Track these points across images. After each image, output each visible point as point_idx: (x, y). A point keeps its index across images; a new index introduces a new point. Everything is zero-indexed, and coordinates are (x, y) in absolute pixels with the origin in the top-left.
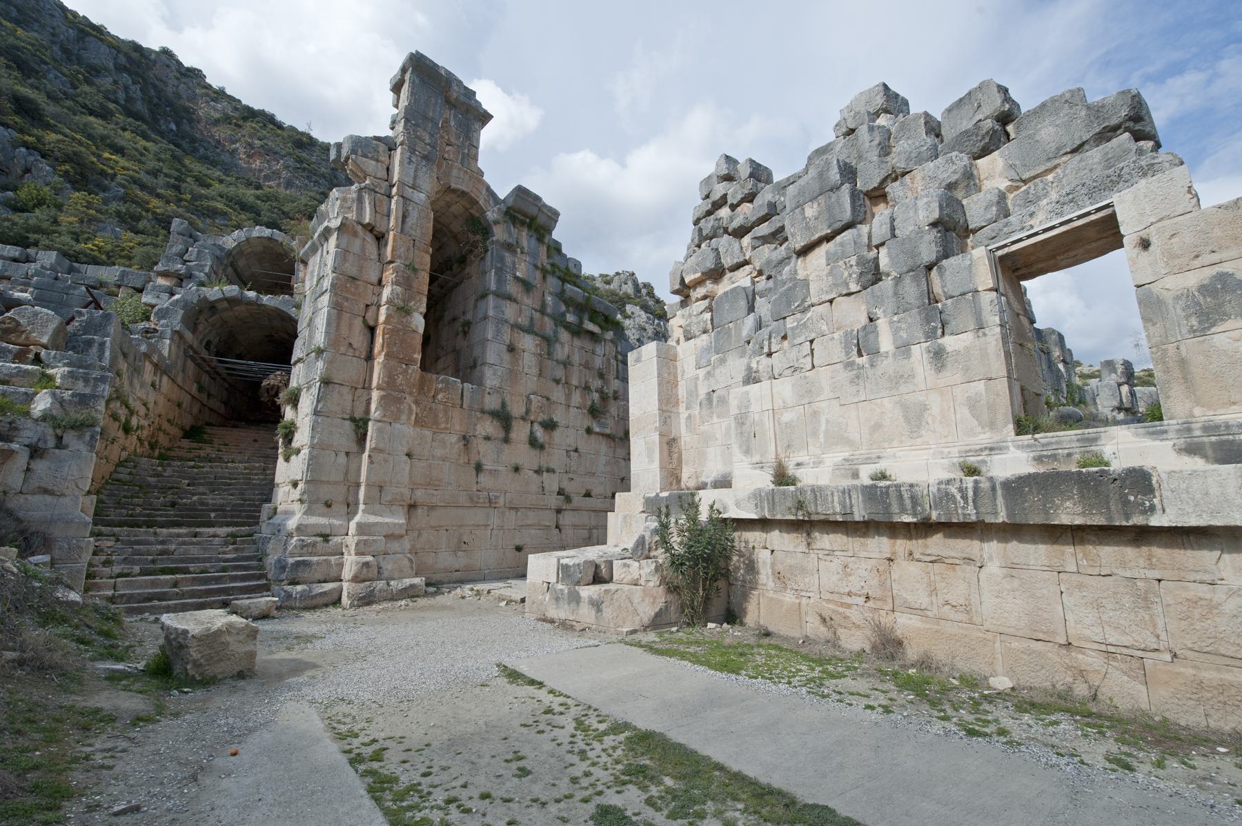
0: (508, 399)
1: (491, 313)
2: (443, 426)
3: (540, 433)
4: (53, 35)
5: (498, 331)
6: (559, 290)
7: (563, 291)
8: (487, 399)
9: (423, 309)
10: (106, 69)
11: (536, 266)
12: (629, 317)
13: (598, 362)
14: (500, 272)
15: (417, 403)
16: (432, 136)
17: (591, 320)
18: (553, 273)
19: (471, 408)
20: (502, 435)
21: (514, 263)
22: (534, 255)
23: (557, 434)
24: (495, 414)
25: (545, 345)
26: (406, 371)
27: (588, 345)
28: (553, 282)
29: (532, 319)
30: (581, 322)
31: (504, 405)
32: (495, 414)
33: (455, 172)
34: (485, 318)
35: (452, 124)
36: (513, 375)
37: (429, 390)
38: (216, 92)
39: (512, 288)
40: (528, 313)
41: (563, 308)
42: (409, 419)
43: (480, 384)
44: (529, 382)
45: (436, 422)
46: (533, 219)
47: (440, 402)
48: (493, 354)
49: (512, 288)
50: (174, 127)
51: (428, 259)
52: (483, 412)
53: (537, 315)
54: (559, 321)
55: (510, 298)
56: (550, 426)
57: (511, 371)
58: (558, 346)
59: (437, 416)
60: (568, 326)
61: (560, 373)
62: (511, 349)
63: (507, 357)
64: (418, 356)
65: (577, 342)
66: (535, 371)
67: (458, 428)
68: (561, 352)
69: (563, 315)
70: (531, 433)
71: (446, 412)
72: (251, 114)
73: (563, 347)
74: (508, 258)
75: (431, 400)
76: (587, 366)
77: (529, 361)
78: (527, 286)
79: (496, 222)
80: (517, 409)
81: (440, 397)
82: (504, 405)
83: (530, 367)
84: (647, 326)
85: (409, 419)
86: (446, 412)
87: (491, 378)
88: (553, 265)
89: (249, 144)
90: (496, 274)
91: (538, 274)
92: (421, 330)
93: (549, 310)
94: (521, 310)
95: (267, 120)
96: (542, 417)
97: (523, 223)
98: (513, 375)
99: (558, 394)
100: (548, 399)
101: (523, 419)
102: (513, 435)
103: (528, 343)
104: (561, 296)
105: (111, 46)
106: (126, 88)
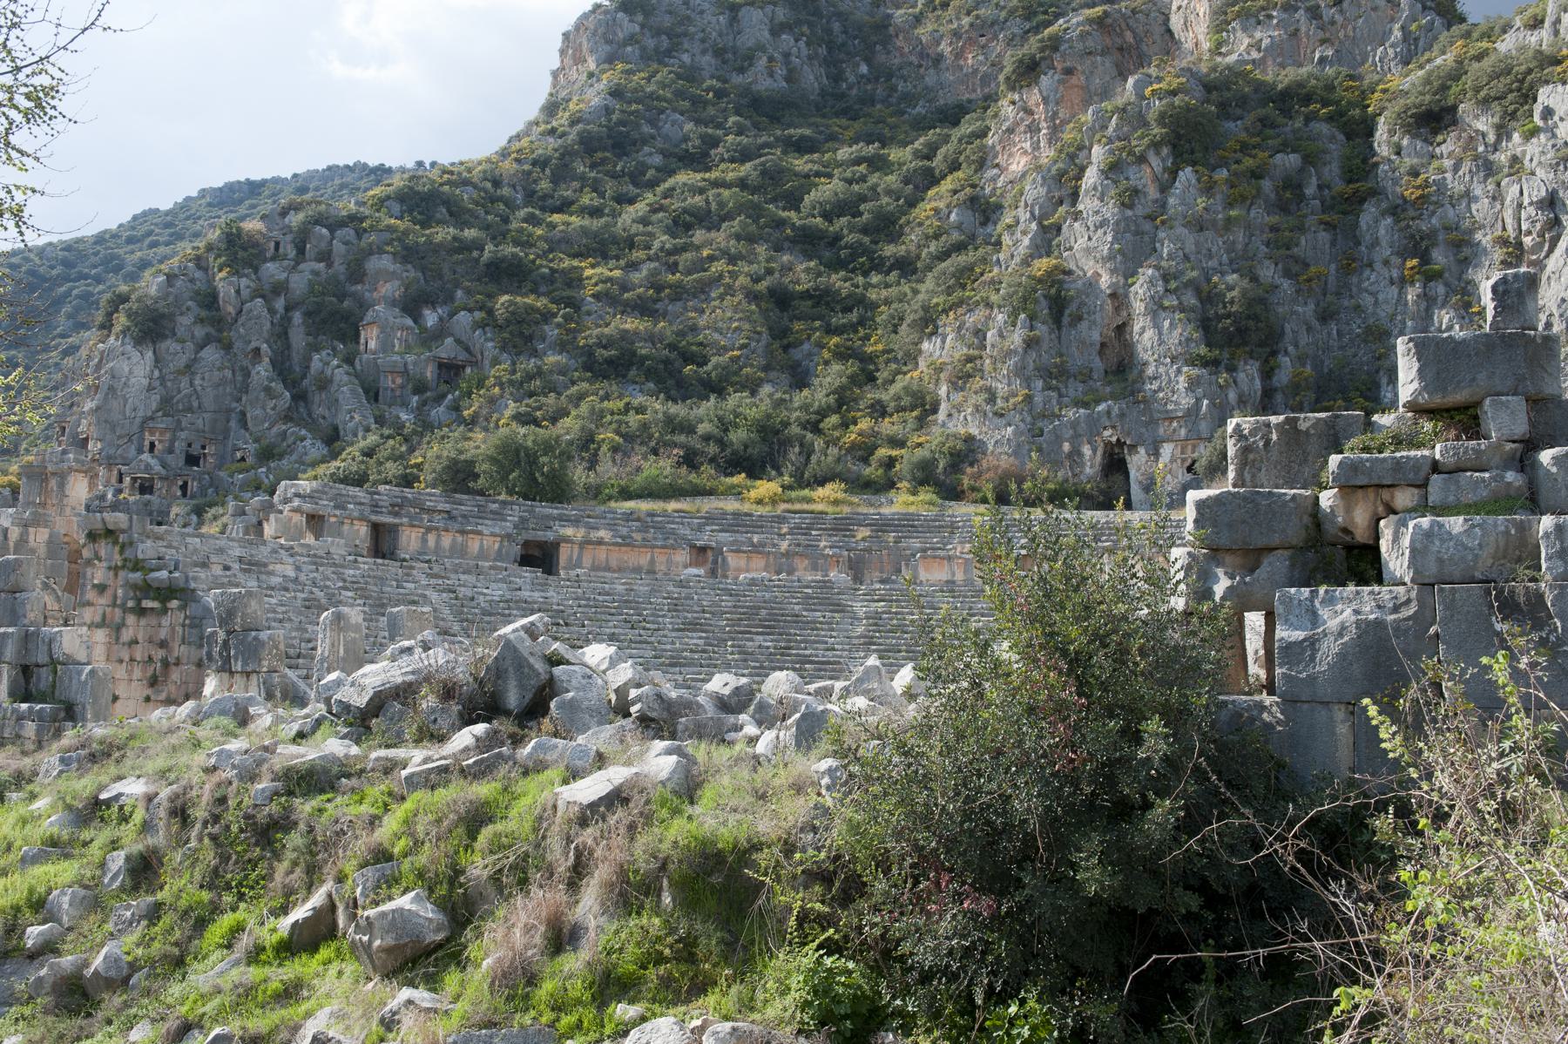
4: (703, 41)
10: (761, 48)
11: (110, 568)
12: (1534, 132)
13: (163, 634)
18: (123, 567)
29: (104, 615)
40: (100, 612)
49: (90, 595)
50: (864, 69)
53: (108, 610)
55: (89, 604)
58: (124, 630)
60: (132, 610)
65: (143, 622)
66: (103, 658)
68: (126, 635)
78: (101, 589)
89: (956, 34)
103: (101, 635)
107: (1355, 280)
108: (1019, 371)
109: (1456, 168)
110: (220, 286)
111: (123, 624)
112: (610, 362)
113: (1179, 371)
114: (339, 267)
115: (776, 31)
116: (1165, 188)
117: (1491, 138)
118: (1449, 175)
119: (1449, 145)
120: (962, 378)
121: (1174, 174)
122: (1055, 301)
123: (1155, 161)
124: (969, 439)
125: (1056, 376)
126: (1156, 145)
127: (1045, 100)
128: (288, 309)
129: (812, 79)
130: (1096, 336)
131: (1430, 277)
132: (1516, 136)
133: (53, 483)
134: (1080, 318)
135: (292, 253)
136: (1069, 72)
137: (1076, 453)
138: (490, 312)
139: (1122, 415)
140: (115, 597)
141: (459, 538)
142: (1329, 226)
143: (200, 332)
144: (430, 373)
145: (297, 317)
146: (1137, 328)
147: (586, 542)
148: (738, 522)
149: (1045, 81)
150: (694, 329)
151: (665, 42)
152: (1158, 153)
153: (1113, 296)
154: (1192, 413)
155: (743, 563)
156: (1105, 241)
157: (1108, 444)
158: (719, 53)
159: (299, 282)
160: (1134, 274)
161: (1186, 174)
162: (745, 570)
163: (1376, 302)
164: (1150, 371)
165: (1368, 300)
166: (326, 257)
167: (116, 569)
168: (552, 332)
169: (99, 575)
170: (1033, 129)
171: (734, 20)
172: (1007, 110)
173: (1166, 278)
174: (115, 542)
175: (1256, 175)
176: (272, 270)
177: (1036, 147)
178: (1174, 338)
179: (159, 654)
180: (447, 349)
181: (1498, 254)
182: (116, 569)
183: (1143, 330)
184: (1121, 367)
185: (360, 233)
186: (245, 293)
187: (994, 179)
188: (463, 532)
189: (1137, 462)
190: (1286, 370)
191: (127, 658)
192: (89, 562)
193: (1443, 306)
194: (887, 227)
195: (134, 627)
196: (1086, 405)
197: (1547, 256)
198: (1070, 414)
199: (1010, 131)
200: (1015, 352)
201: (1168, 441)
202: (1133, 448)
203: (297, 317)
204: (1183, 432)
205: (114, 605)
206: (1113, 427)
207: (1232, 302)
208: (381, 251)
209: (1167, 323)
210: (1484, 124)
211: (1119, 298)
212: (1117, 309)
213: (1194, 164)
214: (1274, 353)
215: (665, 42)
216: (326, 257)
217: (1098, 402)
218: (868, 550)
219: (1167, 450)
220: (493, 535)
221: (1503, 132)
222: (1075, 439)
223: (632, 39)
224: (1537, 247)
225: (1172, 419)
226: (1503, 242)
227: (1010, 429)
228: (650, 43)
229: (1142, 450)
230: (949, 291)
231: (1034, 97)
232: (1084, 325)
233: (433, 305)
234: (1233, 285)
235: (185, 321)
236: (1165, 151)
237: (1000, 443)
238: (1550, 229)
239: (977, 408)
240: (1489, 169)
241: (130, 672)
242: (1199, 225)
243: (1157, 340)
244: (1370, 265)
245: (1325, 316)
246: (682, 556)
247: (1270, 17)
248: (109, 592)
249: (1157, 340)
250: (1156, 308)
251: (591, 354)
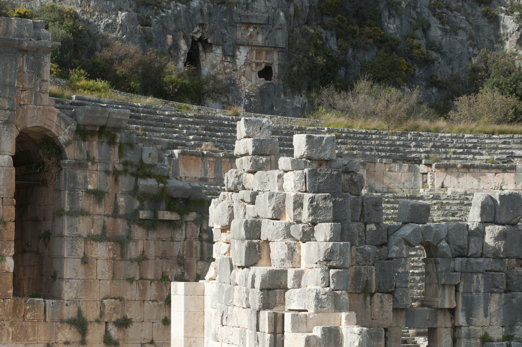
0: (83, 308)
1: (66, 233)
2: (31, 339)
3: (114, 332)
5: (73, 248)
6: (131, 188)
7: (136, 187)
8: (66, 310)
9: (12, 253)
11: (107, 172)
13: (178, 248)
14: (73, 191)
15: (12, 324)
16: (10, 99)
17: (169, 208)
18: (125, 172)
19: (52, 321)
20: (78, 338)
21: (85, 178)
22: (105, 161)
23: (131, 331)
24: (71, 322)
25: (118, 248)
26: (3, 304)
27: (165, 234)
28: (126, 182)
29: (104, 227)
30: (156, 215)
31: (80, 312)
32: (71, 322)
33: (30, 114)
34: (62, 236)
35: (25, 69)
36: (87, 284)
37: (20, 312)
39: (85, 203)
40: (99, 222)
41: (137, 204)
42: (8, 339)
43: (59, 298)
44: (104, 286)
45: (27, 337)
46: (102, 128)
47: (29, 320)
48: (70, 269)
49: (85, 203)
51: (13, 209)
52: (62, 321)
53: (109, 221)
54: (132, 218)
55: (83, 213)
56: (124, 323)
57: (85, 281)
58: (132, 246)
59: (27, 331)
60: (142, 223)
61: (134, 271)
62: (85, 261)
63: (81, 269)
64: (11, 291)
65: (153, 235)
66: (108, 275)
67: (43, 338)
68: (134, 250)
69: (136, 212)
70: (106, 331)
71: (33, 327)
73: (136, 242)
74: (80, 174)
75: (21, 320)
76: (164, 256)
77: (102, 268)
78: (98, 195)
79: (68, 143)
80: (91, 314)
81: (28, 316)
82: (80, 312)
83: (103, 273)
85: (8, 339)
86: (33, 327)
87: (68, 292)
88: (125, 164)
90: (69, 194)
91: (110, 179)
92: (12, 270)
93: (121, 212)
94: (93, 221)
96: (115, 317)
97: (92, 134)
98: (87, 284)
99: (132, 292)
100: (121, 299)
101: (98, 321)
102: (89, 337)
103: (101, 251)
104: (134, 192)
111: (129, 237)
140: (116, 207)
167: (116, 174)
174: (111, 142)
182: (116, 174)
189: (212, 62)
202: (208, 46)
204: (260, 38)
205: (115, 214)
219: (242, 55)
227: (122, 15)
241: (143, 292)
248: (108, 200)
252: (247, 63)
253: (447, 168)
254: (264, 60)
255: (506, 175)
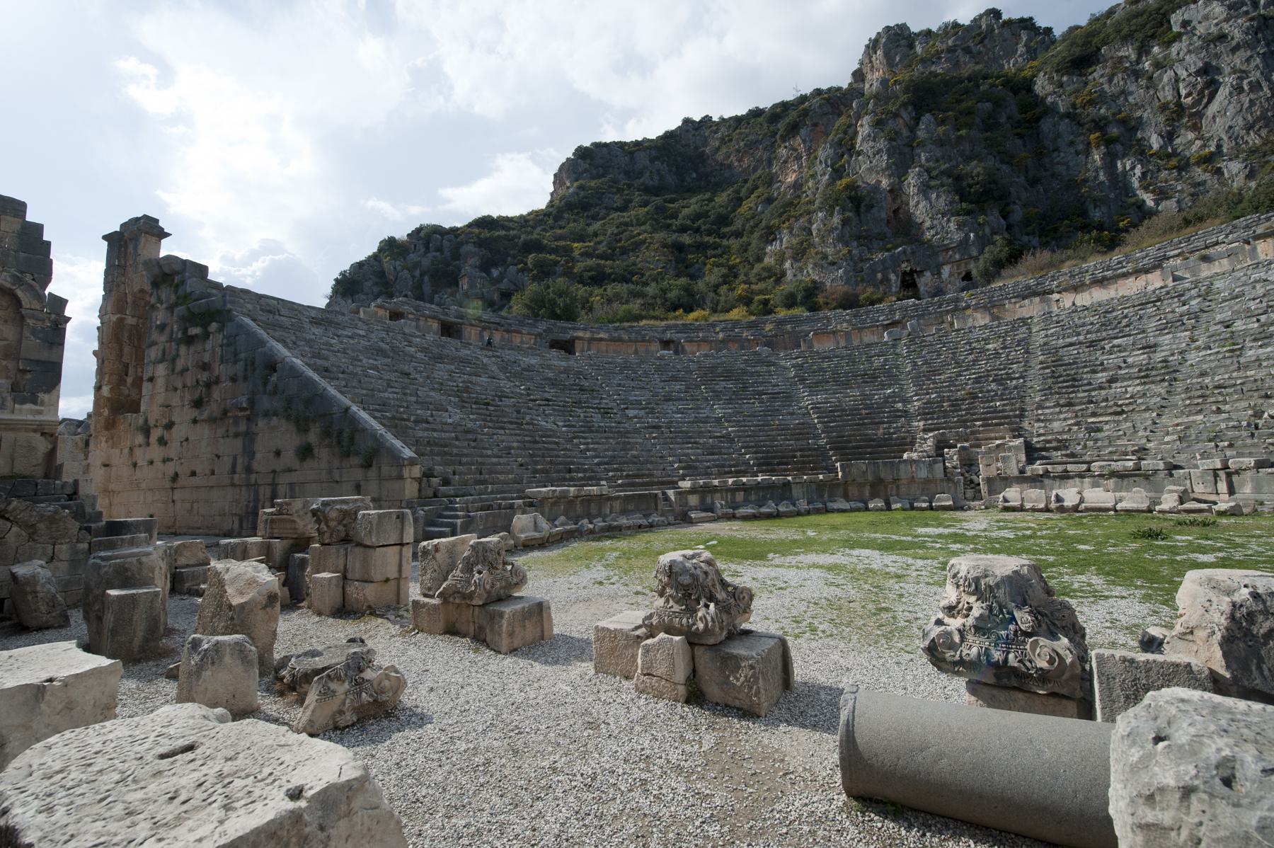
38: (717, 124)
40: (161, 348)
50: (694, 175)
53: (167, 345)
55: (154, 343)
65: (192, 349)
68: (180, 364)
72: (737, 121)
78: (162, 328)
84: (1226, 28)
89: (738, 151)
95: (756, 113)
105: (650, 148)
106: (658, 170)
107: (1046, 160)
108: (840, 239)
109: (1110, 81)
110: (385, 265)
112: (592, 278)
113: (949, 221)
114: (447, 253)
115: (652, 161)
116: (913, 130)
117: (1133, 57)
118: (1106, 87)
119: (1098, 74)
120: (800, 253)
121: (917, 120)
122: (856, 201)
123: (904, 114)
124: (814, 282)
125: (865, 239)
126: (904, 105)
127: (804, 142)
128: (422, 275)
129: (671, 179)
130: (883, 215)
131: (1109, 142)
132: (1156, 49)
133: (131, 248)
134: (872, 207)
135: (422, 250)
136: (815, 125)
137: (886, 280)
138: (526, 264)
139: (913, 253)
141: (506, 336)
142: (1020, 136)
143: (376, 290)
144: (496, 297)
145: (426, 278)
146: (912, 203)
147: (592, 340)
148: (685, 328)
149: (803, 132)
150: (634, 264)
151: (601, 171)
152: (906, 109)
153: (891, 191)
154: (963, 245)
155: (695, 349)
156: (884, 160)
157: (905, 273)
158: (627, 173)
159: (426, 262)
160: (906, 173)
161: (927, 117)
162: (698, 353)
163: (1068, 168)
164: (928, 224)
165: (1061, 169)
166: (440, 249)
168: (559, 269)
169: (160, 316)
170: (798, 158)
171: (632, 158)
172: (783, 152)
173: (928, 171)
175: (969, 112)
176: (413, 257)
177: (800, 167)
178: (942, 203)
179: (204, 376)
180: (504, 285)
181: (1161, 118)
183: (918, 203)
184: (904, 227)
185: (456, 237)
186: (399, 268)
187: (779, 188)
188: (508, 331)
190: (1018, 213)
191: (180, 386)
192: (153, 307)
193: (1124, 156)
194: (724, 220)
195: (186, 357)
196: (888, 250)
197: (1206, 106)
198: (879, 256)
199: (785, 162)
200: (836, 228)
201: (947, 263)
202: (921, 273)
203: (426, 278)
206: (908, 261)
207: (978, 175)
208: (467, 243)
209: (934, 196)
210: (1129, 51)
211: (895, 191)
212: (894, 199)
213: (930, 111)
214: (1007, 205)
215: (601, 171)
216: (440, 249)
217: (897, 247)
218: (775, 336)
219: (946, 271)
220: (529, 334)
221: (1143, 50)
222: (884, 271)
223: (586, 171)
224: (1197, 103)
225: (948, 250)
226: (1164, 107)
227: (840, 271)
228: (594, 172)
229: (928, 274)
230: (780, 215)
231: (797, 141)
232: (875, 210)
233: (496, 265)
234: (976, 169)
235: (368, 284)
236: (910, 108)
237: (834, 281)
238: (1207, 88)
239: (815, 265)
240: (1137, 74)
241: (182, 398)
242: (940, 143)
243: (926, 209)
244: (1057, 149)
245: (1033, 182)
246: (655, 346)
247: (940, 58)
248: (168, 329)
249: (926, 209)
250: (925, 189)
251: (581, 276)
252: (951, 275)
253: (1076, 289)
254: (963, 270)
255: (1149, 276)
